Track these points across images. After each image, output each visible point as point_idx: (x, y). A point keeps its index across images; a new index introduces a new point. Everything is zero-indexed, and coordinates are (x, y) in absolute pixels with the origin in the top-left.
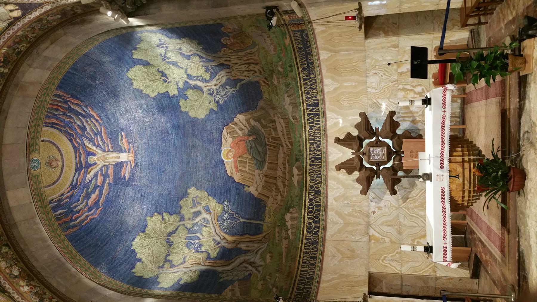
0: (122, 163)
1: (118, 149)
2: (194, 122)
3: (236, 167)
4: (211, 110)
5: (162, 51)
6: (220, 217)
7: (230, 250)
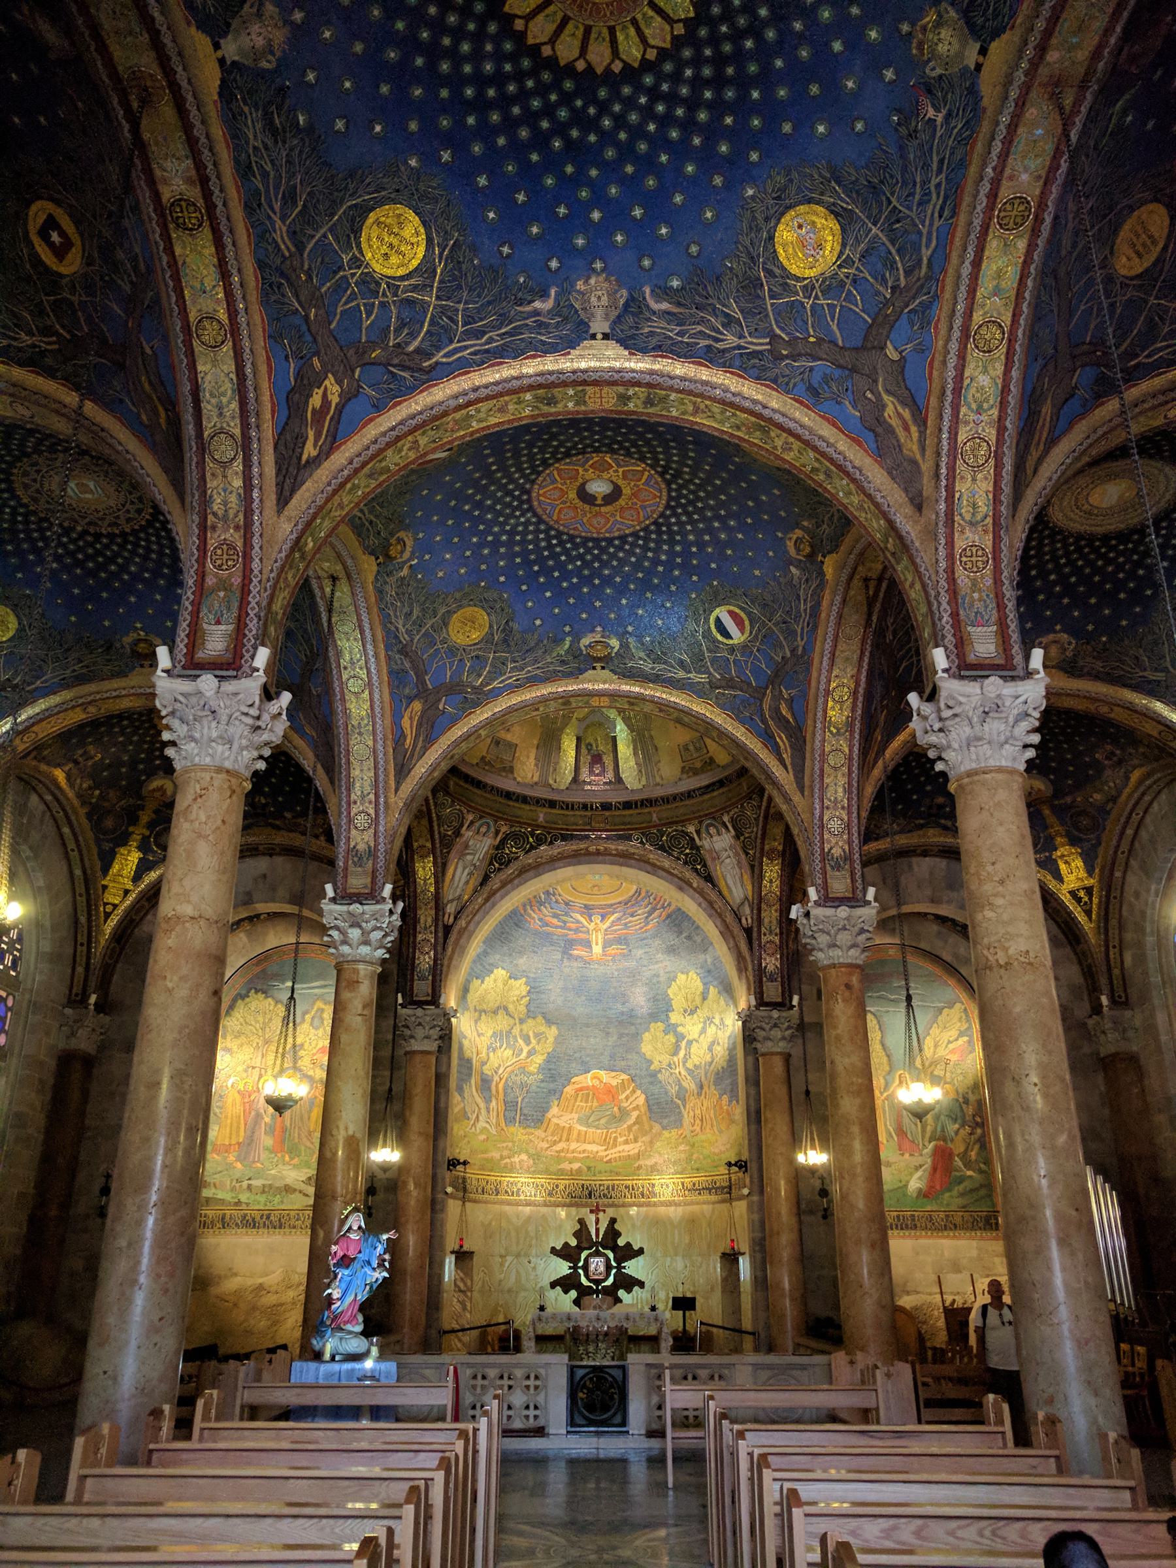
0: (590, 947)
1: (607, 944)
2: (636, 1037)
3: (581, 1089)
4: (650, 1062)
5: (717, 1021)
6: (523, 1070)
7: (489, 1089)
